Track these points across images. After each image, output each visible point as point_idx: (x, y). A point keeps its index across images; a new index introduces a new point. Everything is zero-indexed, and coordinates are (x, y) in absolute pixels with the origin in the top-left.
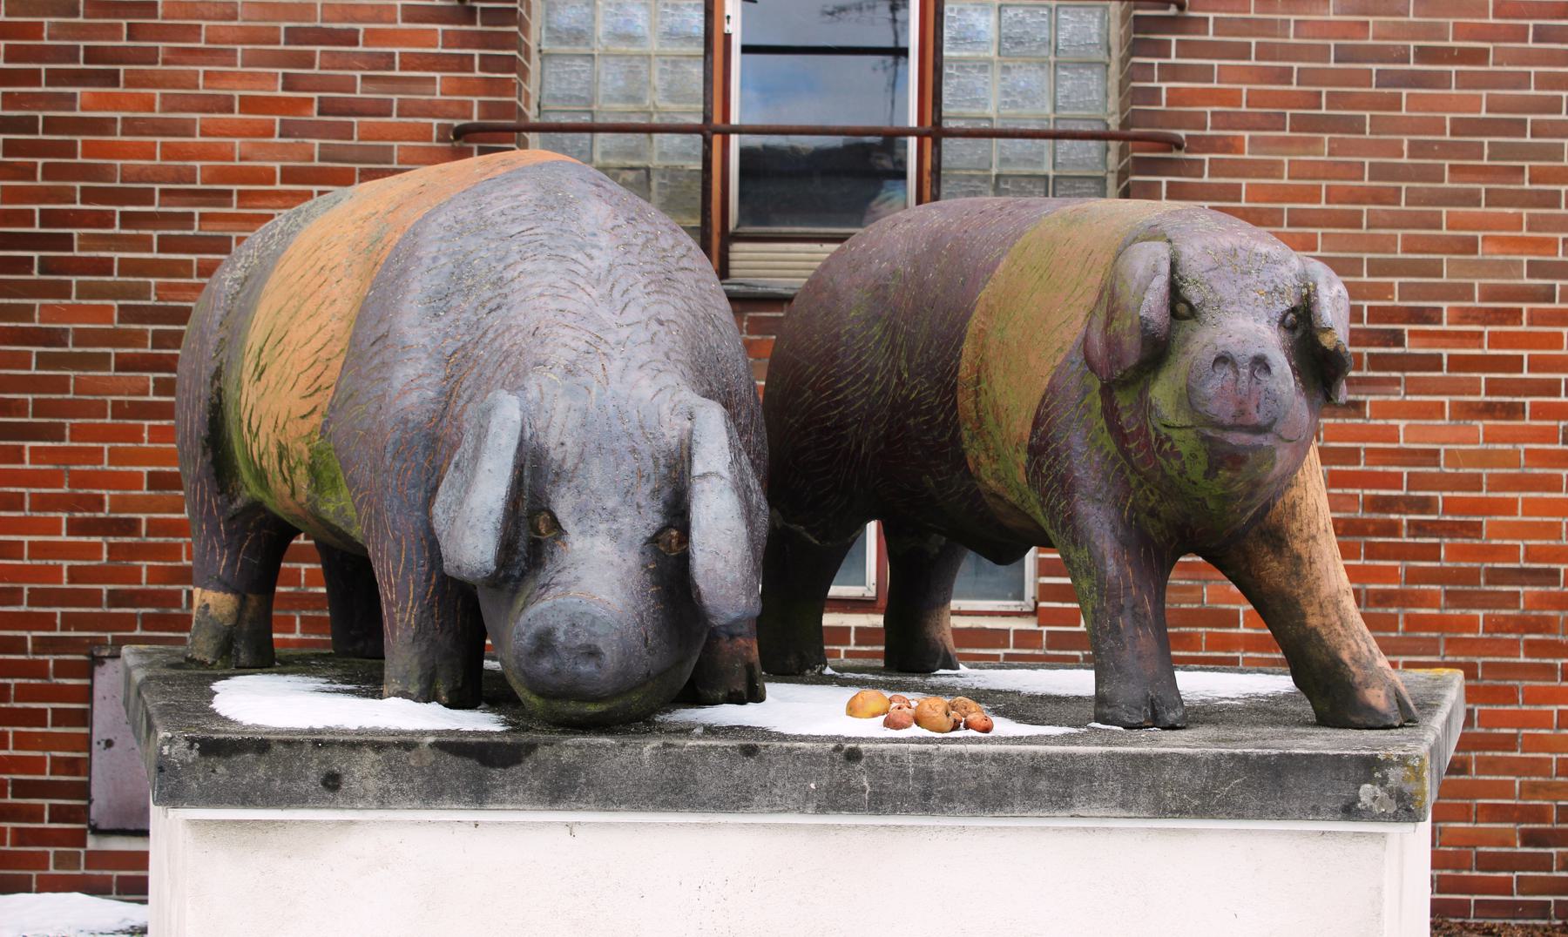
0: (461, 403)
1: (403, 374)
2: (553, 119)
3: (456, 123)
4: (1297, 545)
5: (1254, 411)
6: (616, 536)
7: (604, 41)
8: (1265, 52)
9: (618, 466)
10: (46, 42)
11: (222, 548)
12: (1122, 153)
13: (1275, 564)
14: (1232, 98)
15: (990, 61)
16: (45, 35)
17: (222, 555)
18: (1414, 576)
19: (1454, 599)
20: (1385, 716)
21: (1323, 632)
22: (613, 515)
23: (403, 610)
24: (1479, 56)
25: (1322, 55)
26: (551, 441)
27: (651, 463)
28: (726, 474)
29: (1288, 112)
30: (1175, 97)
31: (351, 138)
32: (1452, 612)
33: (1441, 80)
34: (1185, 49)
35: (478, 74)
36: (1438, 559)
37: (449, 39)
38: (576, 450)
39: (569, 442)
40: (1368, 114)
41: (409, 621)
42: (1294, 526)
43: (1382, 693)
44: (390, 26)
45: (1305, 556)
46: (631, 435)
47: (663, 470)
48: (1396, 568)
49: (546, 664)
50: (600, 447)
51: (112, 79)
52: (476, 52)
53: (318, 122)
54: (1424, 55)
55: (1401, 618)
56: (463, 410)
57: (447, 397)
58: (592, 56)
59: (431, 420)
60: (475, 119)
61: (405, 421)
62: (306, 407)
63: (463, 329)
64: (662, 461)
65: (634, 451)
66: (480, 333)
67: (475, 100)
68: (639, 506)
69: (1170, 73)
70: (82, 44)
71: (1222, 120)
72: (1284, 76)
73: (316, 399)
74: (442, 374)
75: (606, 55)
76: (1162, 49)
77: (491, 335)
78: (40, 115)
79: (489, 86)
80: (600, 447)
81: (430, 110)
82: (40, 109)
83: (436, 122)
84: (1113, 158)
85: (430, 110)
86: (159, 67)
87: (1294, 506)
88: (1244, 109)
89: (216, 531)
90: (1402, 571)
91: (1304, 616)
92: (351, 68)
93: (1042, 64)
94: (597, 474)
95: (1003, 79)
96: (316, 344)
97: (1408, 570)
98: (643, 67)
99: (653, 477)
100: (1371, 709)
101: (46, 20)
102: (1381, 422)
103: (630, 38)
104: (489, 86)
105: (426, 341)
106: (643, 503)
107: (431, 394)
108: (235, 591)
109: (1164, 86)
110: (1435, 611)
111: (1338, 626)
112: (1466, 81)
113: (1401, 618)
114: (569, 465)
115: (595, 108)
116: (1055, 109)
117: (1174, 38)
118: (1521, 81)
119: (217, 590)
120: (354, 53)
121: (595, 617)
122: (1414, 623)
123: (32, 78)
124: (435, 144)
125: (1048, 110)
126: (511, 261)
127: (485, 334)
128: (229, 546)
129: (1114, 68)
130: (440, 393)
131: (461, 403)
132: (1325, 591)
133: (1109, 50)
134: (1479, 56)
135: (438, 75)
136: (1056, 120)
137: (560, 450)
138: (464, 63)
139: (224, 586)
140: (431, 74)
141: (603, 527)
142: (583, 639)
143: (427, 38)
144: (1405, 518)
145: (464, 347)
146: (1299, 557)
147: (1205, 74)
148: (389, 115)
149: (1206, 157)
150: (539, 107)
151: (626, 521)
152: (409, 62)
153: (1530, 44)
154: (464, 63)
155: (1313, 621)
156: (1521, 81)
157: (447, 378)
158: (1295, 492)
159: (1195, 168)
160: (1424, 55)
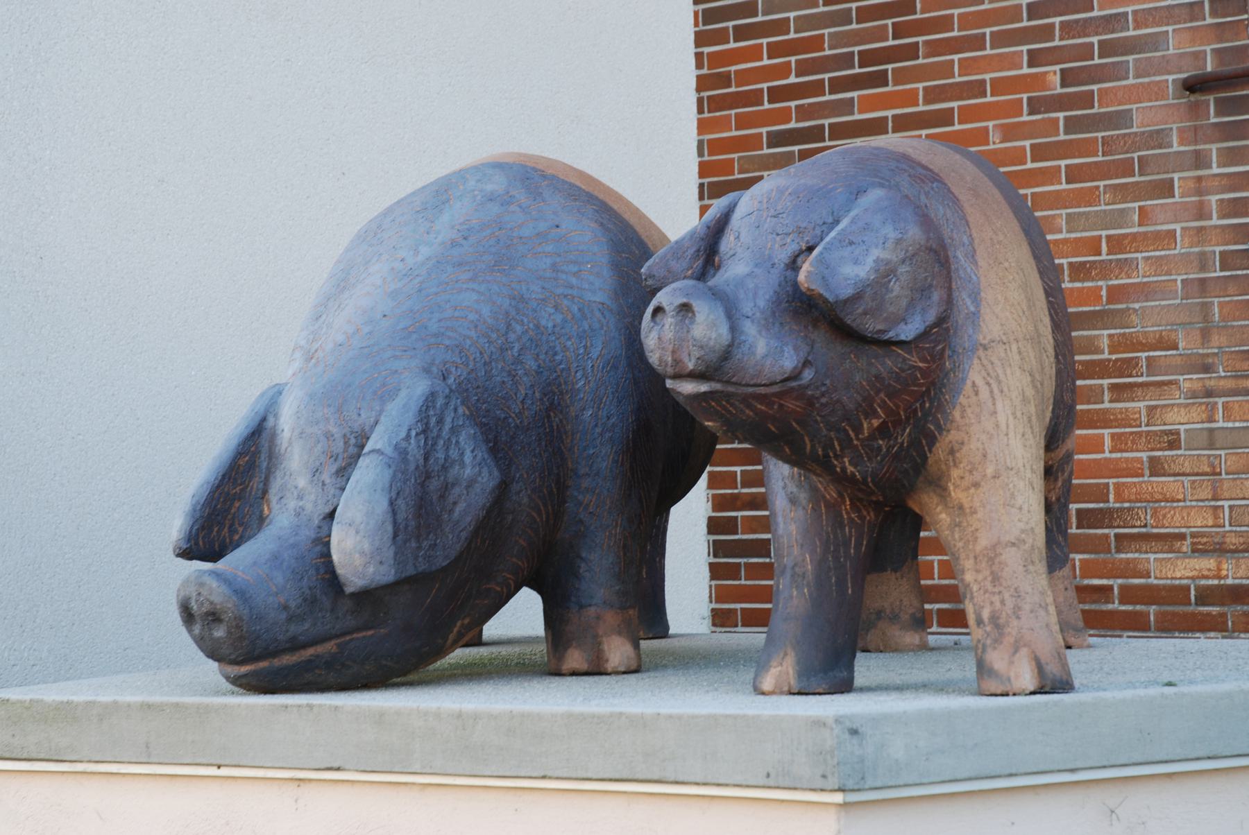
5: (686, 360)
10: (828, 52)
13: (943, 516)
16: (826, 45)
27: (342, 444)
28: (389, 451)
31: (1093, 107)
35: (1209, 21)
42: (955, 473)
45: (966, 505)
51: (881, 79)
53: (1060, 95)
64: (353, 441)
67: (1208, 49)
68: (324, 484)
70: (856, 49)
78: (826, 122)
81: (1164, 66)
82: (826, 117)
83: (1171, 78)
85: (1164, 66)
86: (920, 61)
87: (952, 452)
92: (1088, 36)
99: (340, 457)
101: (826, 31)
106: (328, 481)
120: (1091, 18)
123: (817, 88)
124: (1171, 101)
146: (961, 507)
158: (953, 436)
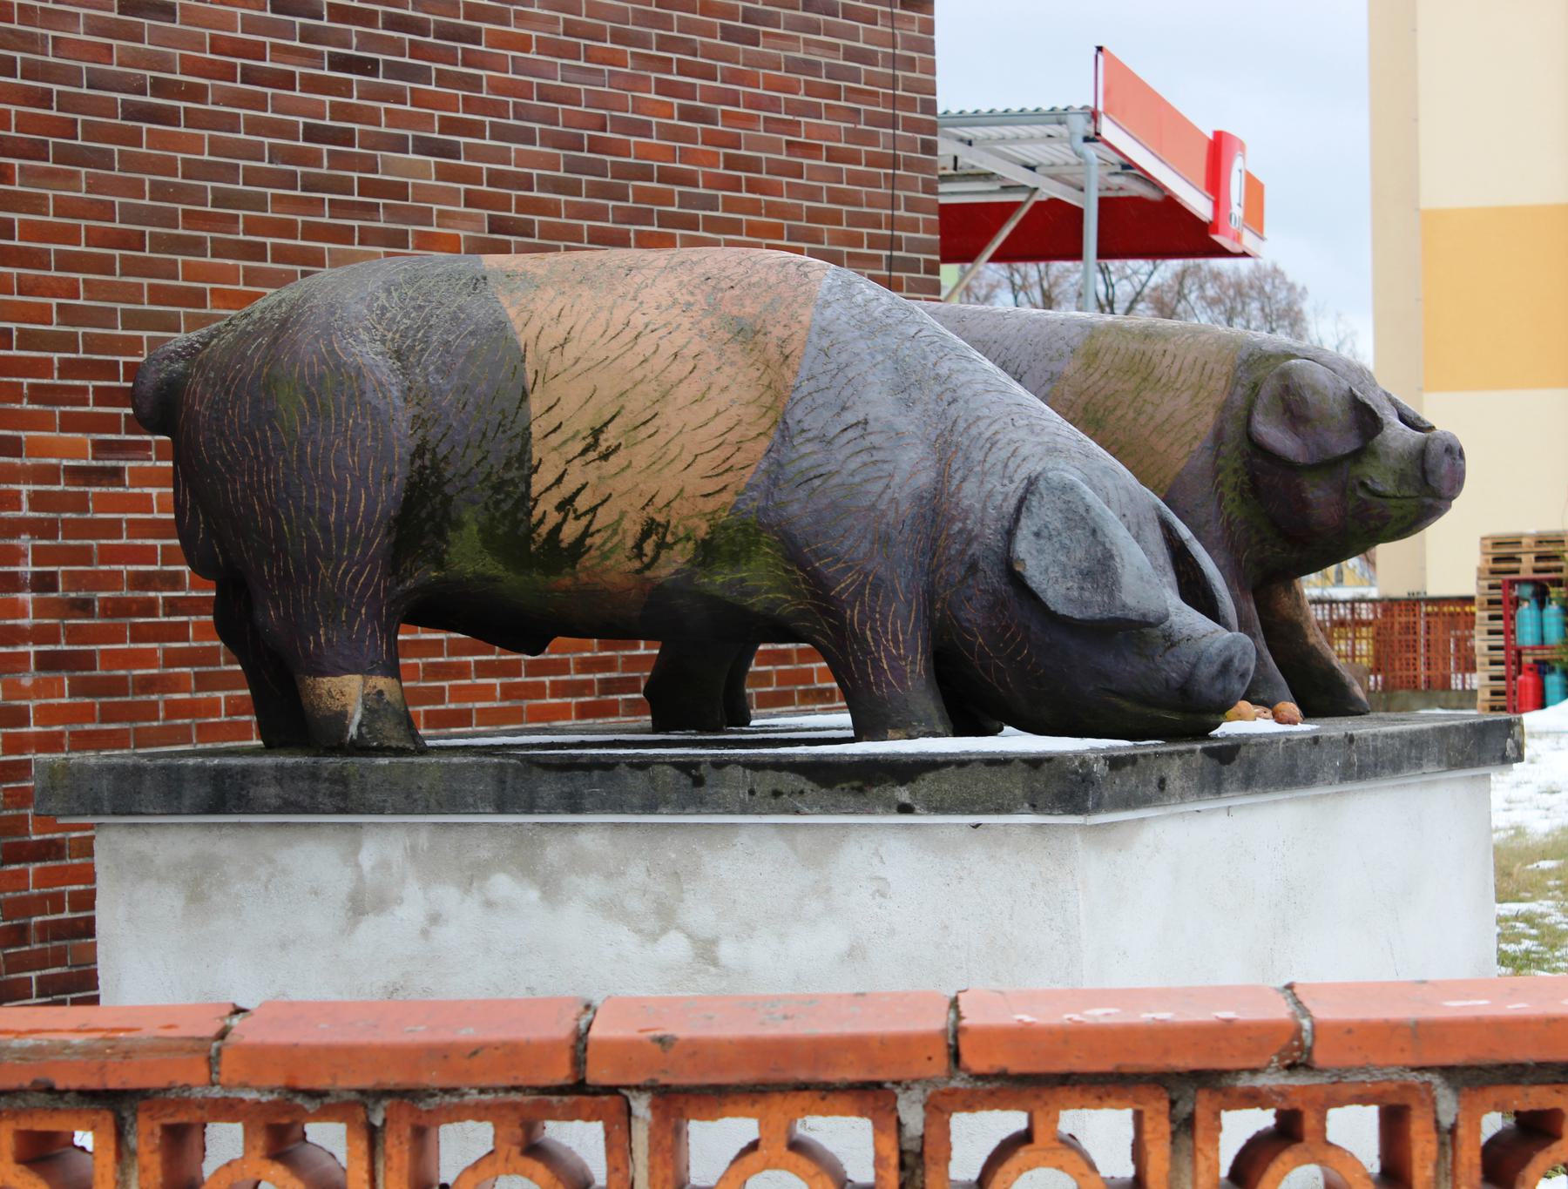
23: (913, 663)
36: (187, 640)
48: (154, 650)
55: (161, 705)
56: (959, 488)
57: (943, 476)
62: (711, 486)
63: (935, 419)
66: (949, 423)
73: (727, 478)
96: (719, 425)
97: (166, 651)
102: (137, 490)
105: (912, 428)
110: (186, 696)
113: (161, 705)
122: (174, 709)
131: (955, 482)
144: (160, 595)
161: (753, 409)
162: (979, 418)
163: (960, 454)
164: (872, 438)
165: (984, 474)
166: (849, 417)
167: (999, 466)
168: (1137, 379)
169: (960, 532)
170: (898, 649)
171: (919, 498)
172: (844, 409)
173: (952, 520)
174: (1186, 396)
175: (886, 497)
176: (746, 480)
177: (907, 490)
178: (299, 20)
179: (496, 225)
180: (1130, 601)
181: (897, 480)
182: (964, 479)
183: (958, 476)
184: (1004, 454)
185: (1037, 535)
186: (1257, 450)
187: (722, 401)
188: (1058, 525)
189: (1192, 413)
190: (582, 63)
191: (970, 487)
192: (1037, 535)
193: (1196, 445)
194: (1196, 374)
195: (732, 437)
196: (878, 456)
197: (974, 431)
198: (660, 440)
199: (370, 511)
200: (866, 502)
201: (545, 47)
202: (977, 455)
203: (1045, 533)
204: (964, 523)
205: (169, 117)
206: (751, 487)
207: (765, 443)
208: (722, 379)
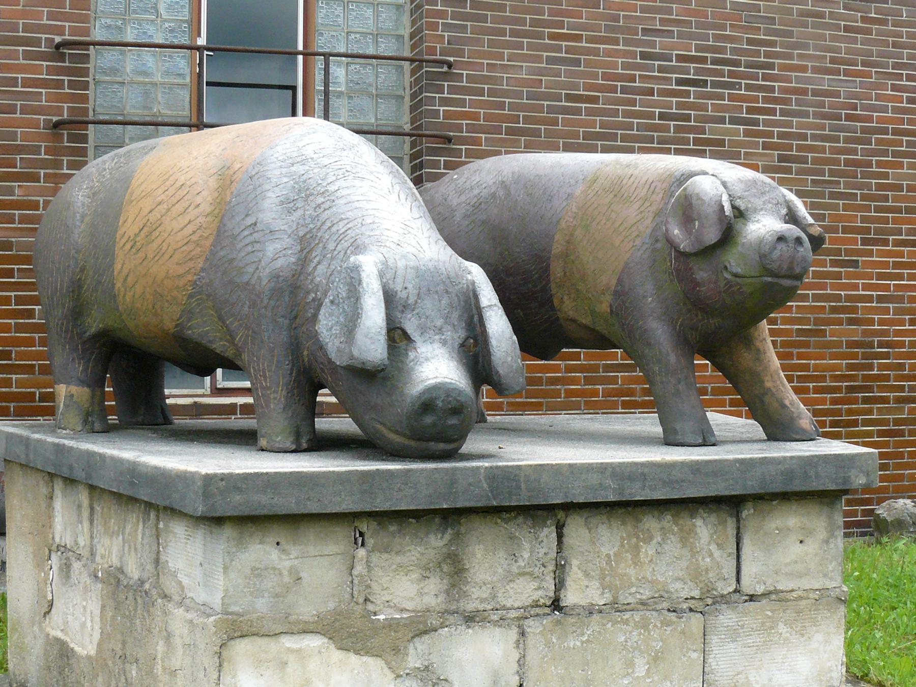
0: (313, 265)
1: (271, 248)
2: (101, 118)
3: (55, 119)
4: (758, 344)
6: (444, 343)
7: (131, 75)
8: (491, 93)
9: (440, 301)
11: (79, 359)
12: (413, 145)
14: (475, 117)
15: (341, 92)
17: (79, 363)
18: (569, 369)
19: (588, 380)
20: (812, 435)
21: (774, 390)
22: (440, 331)
24: (595, 100)
25: (519, 95)
26: (398, 287)
29: (504, 125)
30: (448, 115)
32: (587, 387)
33: (578, 111)
34: (452, 90)
37: (50, 70)
38: (416, 292)
39: (410, 286)
40: (543, 127)
41: (280, 398)
43: (807, 421)
44: (16, 62)
45: (762, 349)
46: (444, 282)
47: (462, 303)
48: (560, 364)
49: (428, 420)
50: (429, 290)
52: (66, 78)
54: (569, 98)
56: (315, 268)
57: (304, 260)
58: (124, 83)
59: (293, 276)
60: (65, 117)
61: (278, 277)
62: (181, 271)
63: (308, 220)
65: (447, 292)
66: (319, 224)
67: (65, 105)
68: (454, 325)
69: (445, 102)
71: (472, 129)
72: (502, 106)
73: (190, 264)
74: (299, 248)
75: (132, 83)
76: (440, 90)
77: (328, 224)
79: (73, 98)
80: (429, 290)
83: (42, 117)
84: (407, 146)
88: (482, 122)
89: (76, 349)
90: (563, 367)
91: (763, 382)
93: (370, 95)
94: (429, 306)
95: (349, 103)
98: (153, 90)
100: (804, 431)
103: (144, 73)
104: (73, 98)
105: (285, 227)
106: (456, 323)
107: (293, 260)
108: (89, 386)
109: (442, 109)
110: (579, 387)
111: (781, 388)
112: (590, 112)
114: (411, 301)
115: (125, 112)
116: (377, 119)
117: (446, 84)
118: (615, 113)
119: (78, 385)
121: (460, 391)
122: (570, 393)
125: (373, 121)
126: (330, 180)
127: (324, 223)
128: (83, 358)
129: (407, 99)
130: (299, 259)
131: (313, 265)
132: (772, 368)
133: (404, 89)
134: (595, 100)
135: (43, 91)
136: (377, 126)
137: (404, 292)
138: (59, 84)
139: (82, 382)
140: (40, 90)
141: (437, 337)
142: (454, 404)
143: (37, 69)
145: (310, 231)
146: (758, 350)
147: (462, 103)
148: (16, 114)
149: (463, 147)
150: (94, 111)
151: (448, 334)
152: (27, 83)
153: (619, 95)
154: (59, 84)
155: (768, 384)
156: (615, 113)
157: (302, 250)
159: (458, 153)
160: (569, 98)
161: (209, 219)
162: (342, 220)
163: (321, 245)
164: (255, 235)
165: (332, 258)
166: (249, 221)
167: (343, 252)
168: (612, 196)
169: (314, 300)
170: (266, 382)
171: (276, 276)
172: (247, 215)
173: (308, 293)
174: (636, 206)
175: (256, 276)
176: (200, 265)
177: (267, 271)
178: (657, 63)
179: (781, 159)
180: (356, 353)
181: (263, 264)
182: (319, 263)
183: (315, 261)
184: (346, 245)
185: (332, 302)
186: (670, 243)
187: (193, 213)
188: (344, 295)
189: (638, 218)
190: (842, 77)
191: (321, 269)
192: (332, 302)
193: (638, 242)
194: (645, 190)
195: (195, 238)
196: (257, 247)
197: (334, 229)
198: (159, 240)
199: (62, 289)
200: (246, 278)
201: (816, 70)
202: (331, 246)
203: (336, 301)
204: (316, 294)
205: (578, 111)
206: (202, 270)
207: (211, 239)
208: (199, 199)
